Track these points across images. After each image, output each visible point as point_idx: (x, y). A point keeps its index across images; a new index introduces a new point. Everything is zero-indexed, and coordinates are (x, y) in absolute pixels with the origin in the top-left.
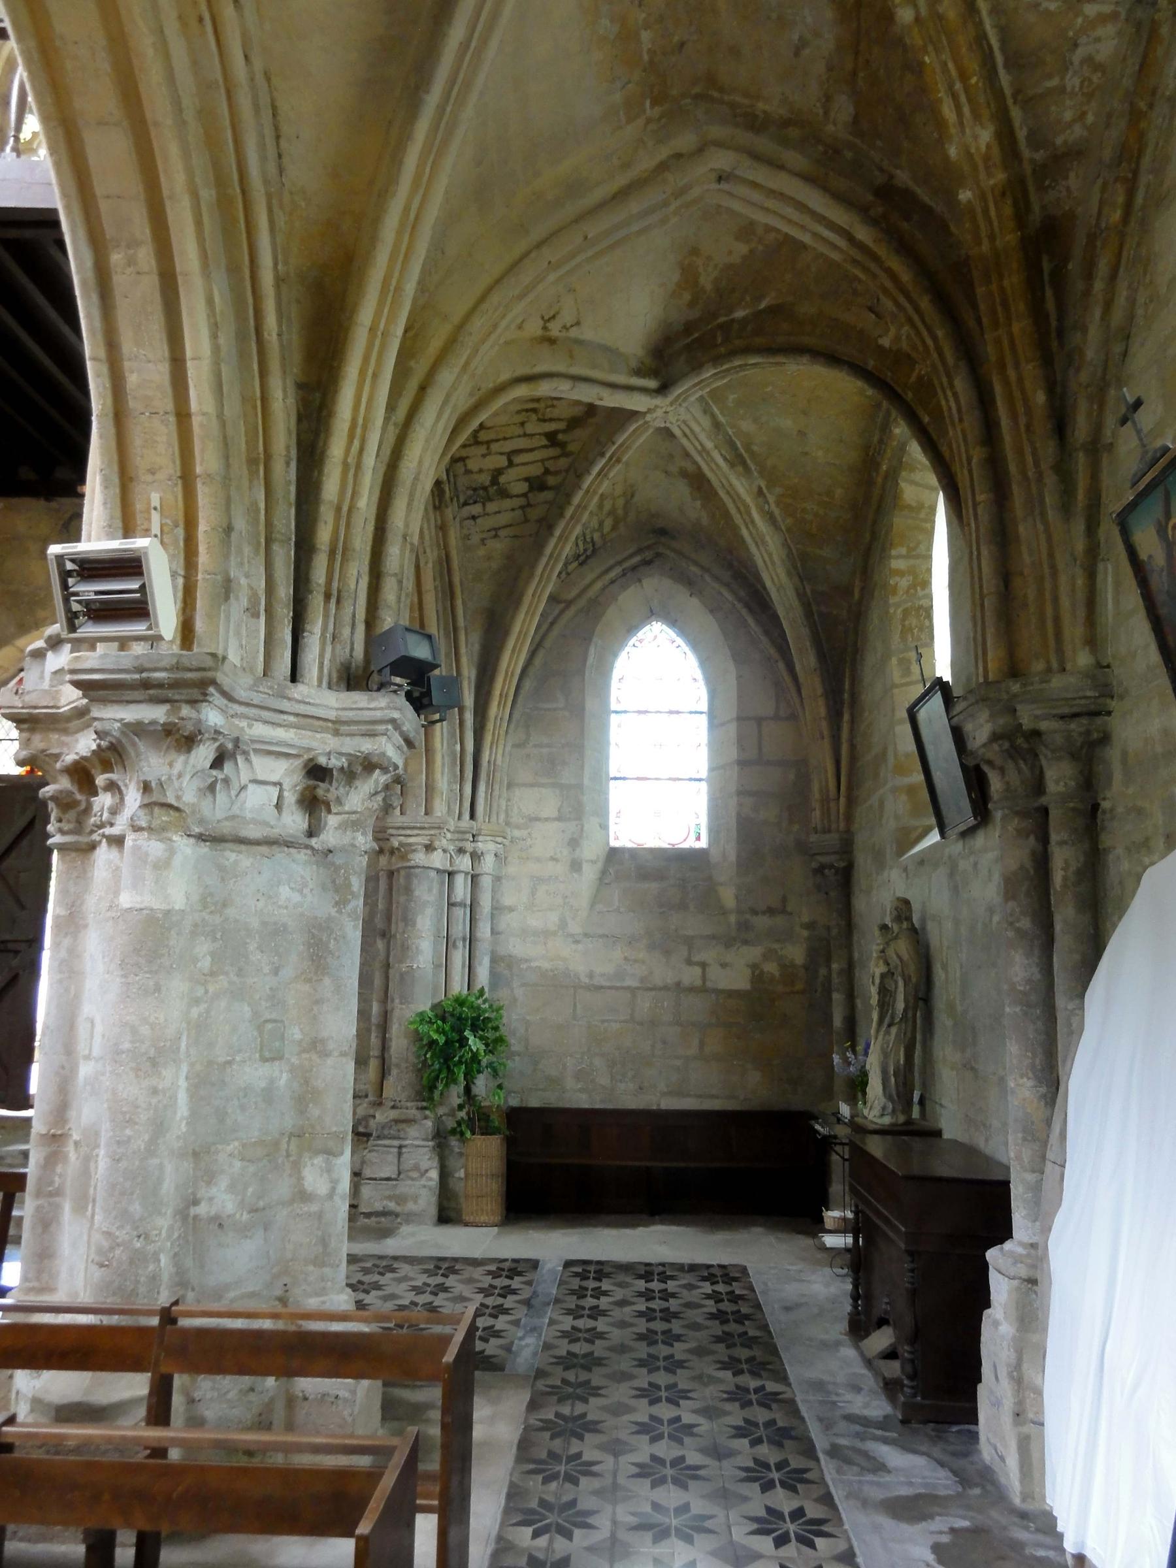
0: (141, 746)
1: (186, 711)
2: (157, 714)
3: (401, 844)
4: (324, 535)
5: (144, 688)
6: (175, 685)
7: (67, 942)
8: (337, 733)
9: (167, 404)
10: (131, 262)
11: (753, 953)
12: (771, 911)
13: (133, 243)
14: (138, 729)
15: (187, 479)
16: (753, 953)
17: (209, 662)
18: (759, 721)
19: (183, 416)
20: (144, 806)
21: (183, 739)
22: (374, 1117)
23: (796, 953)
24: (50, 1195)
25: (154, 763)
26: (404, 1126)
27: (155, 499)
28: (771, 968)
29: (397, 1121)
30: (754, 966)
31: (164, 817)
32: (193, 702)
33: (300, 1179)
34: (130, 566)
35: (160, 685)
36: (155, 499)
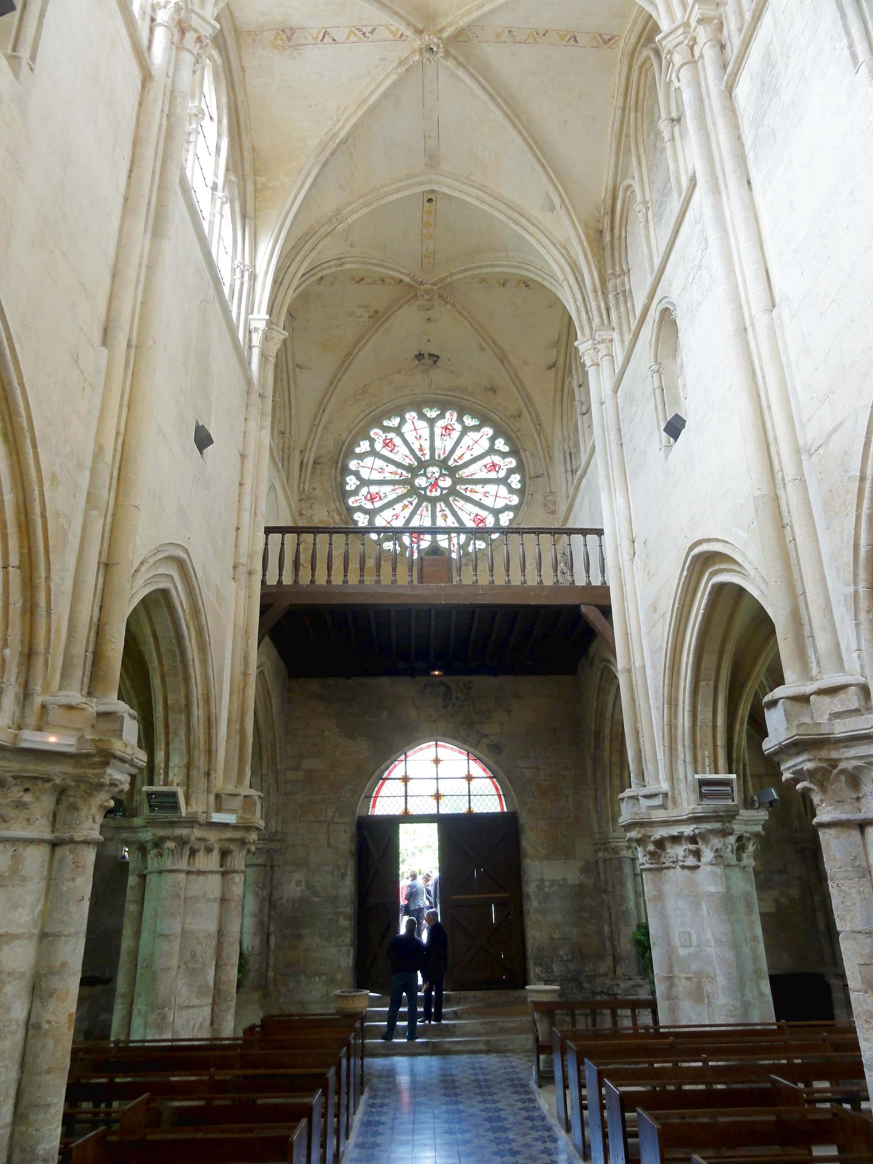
0: (711, 836)
1: (727, 825)
2: (718, 826)
3: (616, 846)
4: (734, 755)
5: (716, 818)
6: (727, 816)
7: (660, 904)
8: (746, 824)
9: (710, 724)
10: (708, 685)
11: (775, 893)
12: (780, 872)
13: (710, 680)
14: (712, 831)
15: (715, 746)
16: (775, 893)
17: (736, 809)
18: (760, 777)
19: (715, 727)
20: (715, 857)
21: (724, 833)
22: (618, 985)
23: (795, 893)
24: (673, 999)
25: (716, 842)
26: (637, 988)
27: (706, 753)
28: (784, 900)
29: (634, 986)
30: (777, 901)
31: (719, 860)
32: (729, 822)
33: (759, 988)
34: (727, 783)
35: (722, 817)
36: (706, 753)
